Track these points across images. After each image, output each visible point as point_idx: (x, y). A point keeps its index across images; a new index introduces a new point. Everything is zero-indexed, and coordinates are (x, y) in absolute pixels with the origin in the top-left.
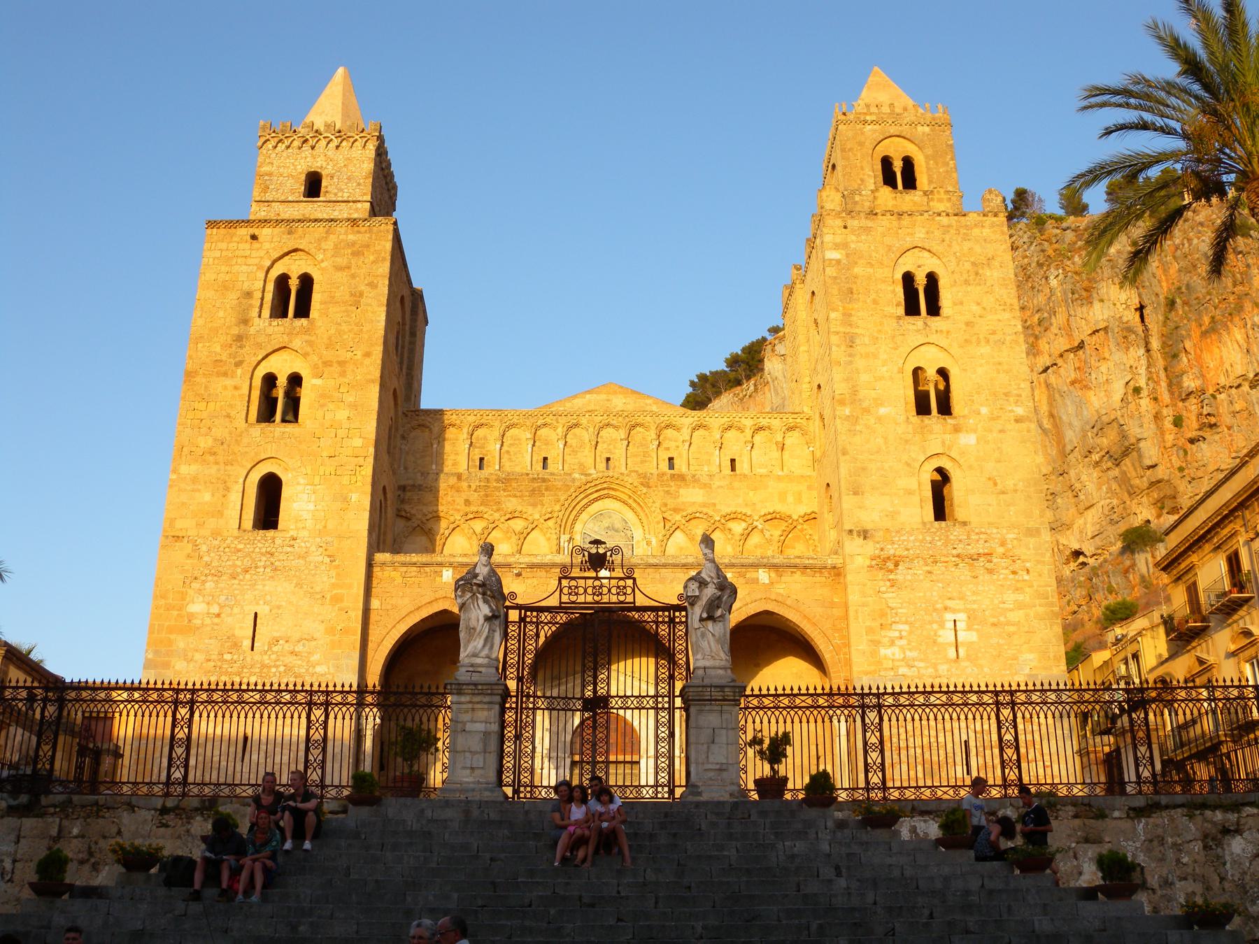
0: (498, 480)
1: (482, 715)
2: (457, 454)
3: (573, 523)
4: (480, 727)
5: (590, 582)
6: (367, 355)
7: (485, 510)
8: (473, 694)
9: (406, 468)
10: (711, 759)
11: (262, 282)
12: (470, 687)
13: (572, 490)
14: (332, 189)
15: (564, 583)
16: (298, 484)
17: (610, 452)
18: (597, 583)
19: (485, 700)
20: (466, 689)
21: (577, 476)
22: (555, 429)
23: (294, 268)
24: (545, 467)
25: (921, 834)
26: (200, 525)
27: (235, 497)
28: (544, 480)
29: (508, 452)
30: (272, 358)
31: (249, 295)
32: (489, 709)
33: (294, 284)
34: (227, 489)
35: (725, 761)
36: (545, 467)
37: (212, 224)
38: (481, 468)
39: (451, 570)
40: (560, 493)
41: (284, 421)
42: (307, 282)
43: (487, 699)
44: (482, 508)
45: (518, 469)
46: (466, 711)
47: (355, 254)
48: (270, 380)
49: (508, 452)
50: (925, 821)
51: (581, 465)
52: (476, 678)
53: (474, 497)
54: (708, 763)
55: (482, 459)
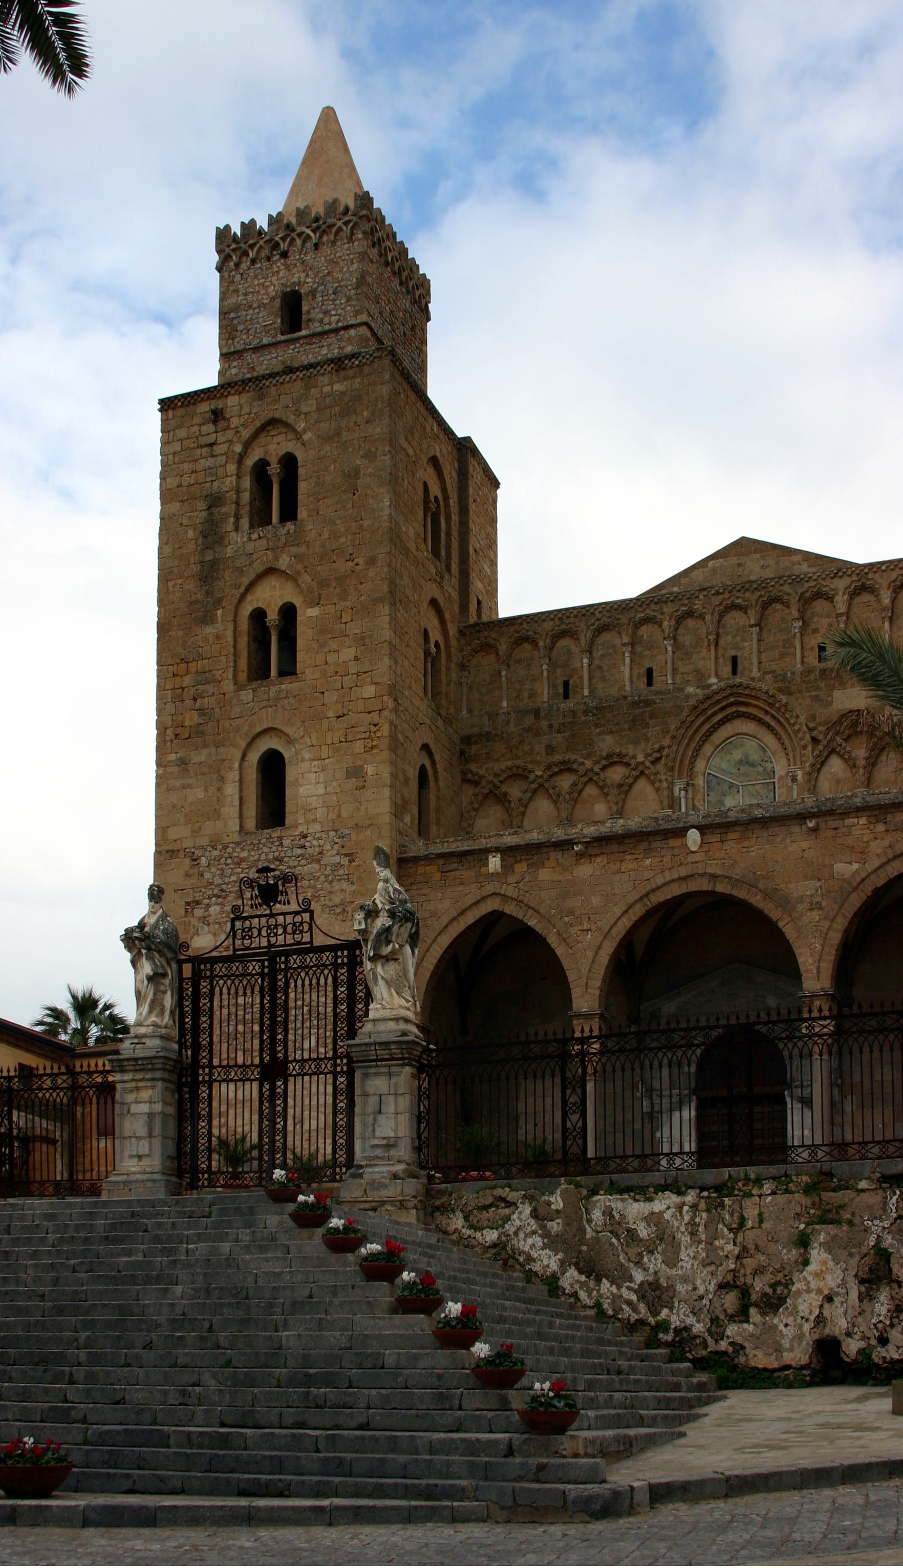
0: (586, 713)
1: (145, 1094)
2: (534, 681)
3: (694, 758)
4: (144, 1108)
7: (573, 757)
8: (136, 1071)
9: (470, 711)
10: (378, 1134)
12: (131, 1063)
13: (685, 714)
17: (739, 649)
19: (147, 1077)
20: (129, 1066)
21: (690, 690)
22: (660, 626)
24: (650, 683)
25: (617, 1216)
28: (648, 703)
29: (600, 668)
32: (153, 1087)
35: (392, 1134)
36: (650, 683)
38: (566, 696)
40: (669, 720)
41: (282, 674)
45: (614, 691)
46: (131, 1091)
49: (600, 668)
50: (623, 1200)
51: (697, 672)
52: (140, 1053)
53: (558, 739)
54: (374, 1138)
55: (566, 684)
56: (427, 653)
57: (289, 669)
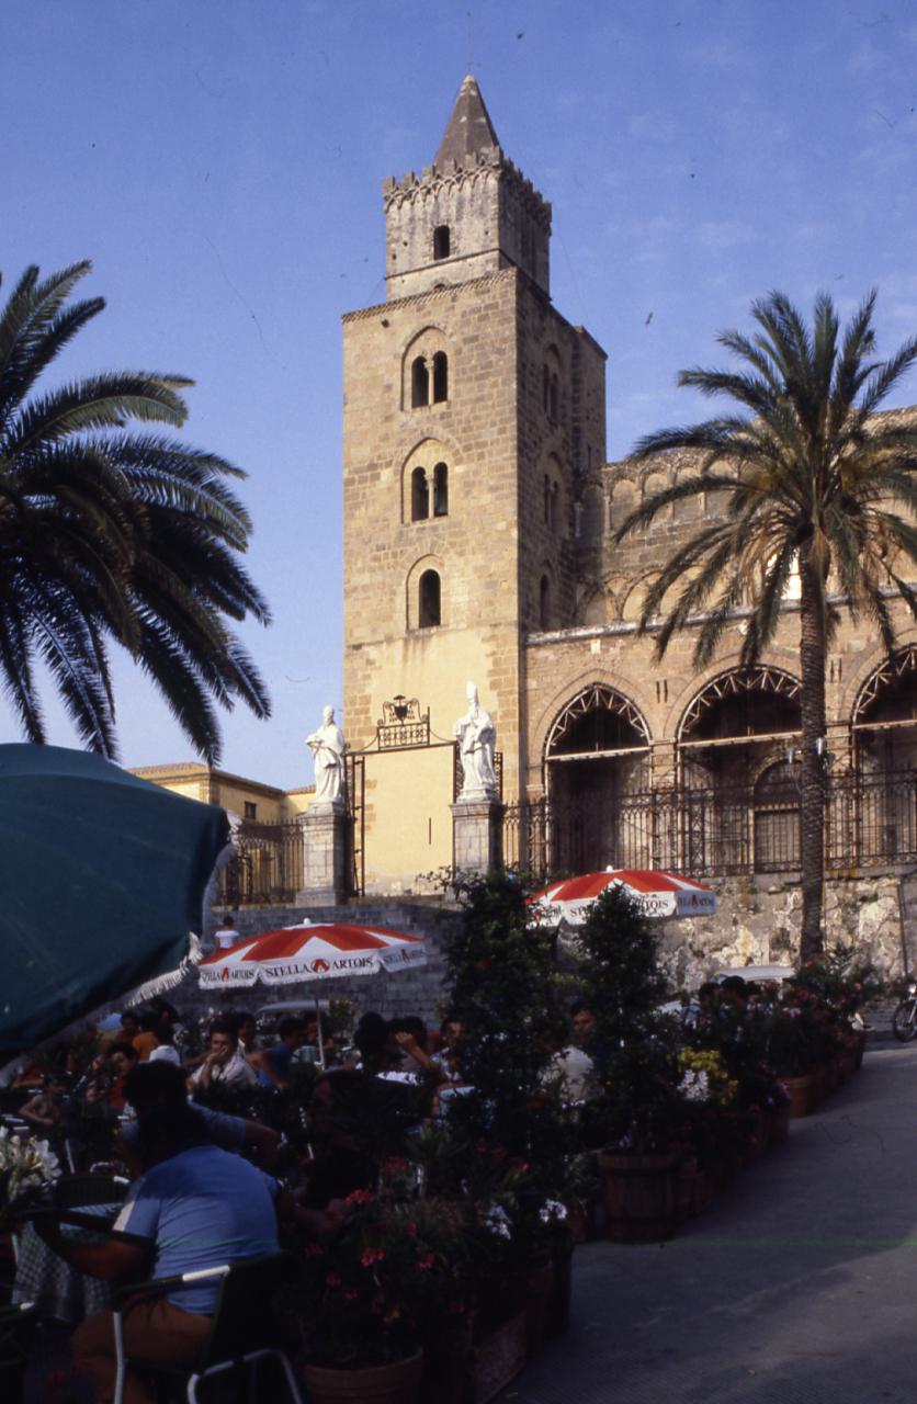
4: (323, 848)
5: (398, 729)
6: (502, 431)
11: (400, 373)
14: (461, 247)
15: (381, 731)
16: (454, 577)
18: (403, 729)
23: (428, 347)
26: (374, 631)
27: (400, 601)
30: (418, 452)
31: (389, 388)
33: (429, 365)
34: (394, 593)
37: (348, 317)
39: (599, 641)
41: (437, 514)
42: (441, 359)
43: (325, 827)
44: (656, 562)
46: (314, 837)
47: (483, 318)
48: (419, 473)
52: (319, 812)
56: (547, 493)
57: (441, 511)
